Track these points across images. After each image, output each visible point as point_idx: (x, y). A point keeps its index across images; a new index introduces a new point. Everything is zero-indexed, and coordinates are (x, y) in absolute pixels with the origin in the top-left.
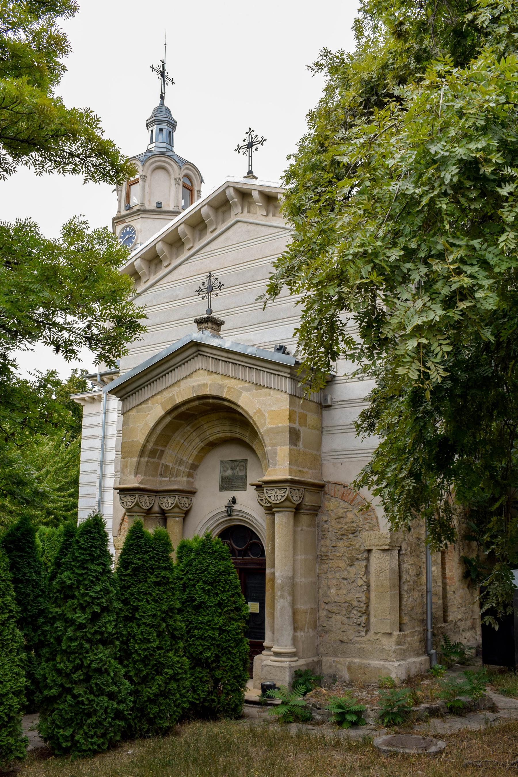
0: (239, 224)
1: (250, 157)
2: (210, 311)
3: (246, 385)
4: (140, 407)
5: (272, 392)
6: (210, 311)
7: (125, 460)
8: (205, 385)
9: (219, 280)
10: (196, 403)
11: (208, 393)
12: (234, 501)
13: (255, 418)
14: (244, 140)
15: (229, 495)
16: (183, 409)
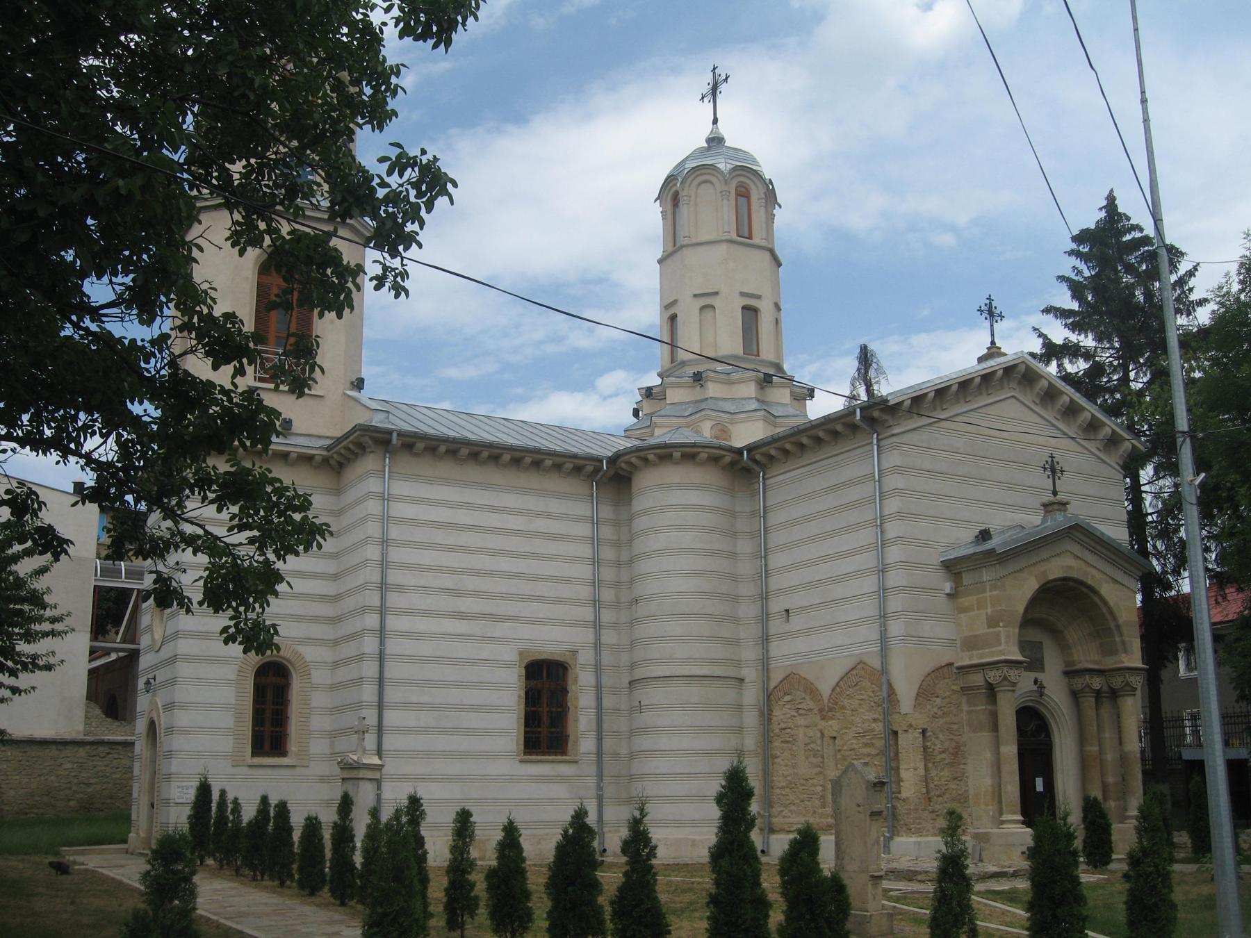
0: (1013, 400)
1: (992, 326)
2: (1055, 493)
3: (1105, 577)
4: (1017, 574)
5: (1125, 589)
6: (1055, 493)
7: (1007, 629)
8: (1070, 568)
9: (1061, 464)
10: (1059, 583)
11: (1075, 576)
12: (1036, 681)
13: (1115, 610)
14: (996, 308)
15: (1032, 675)
16: (1048, 585)
